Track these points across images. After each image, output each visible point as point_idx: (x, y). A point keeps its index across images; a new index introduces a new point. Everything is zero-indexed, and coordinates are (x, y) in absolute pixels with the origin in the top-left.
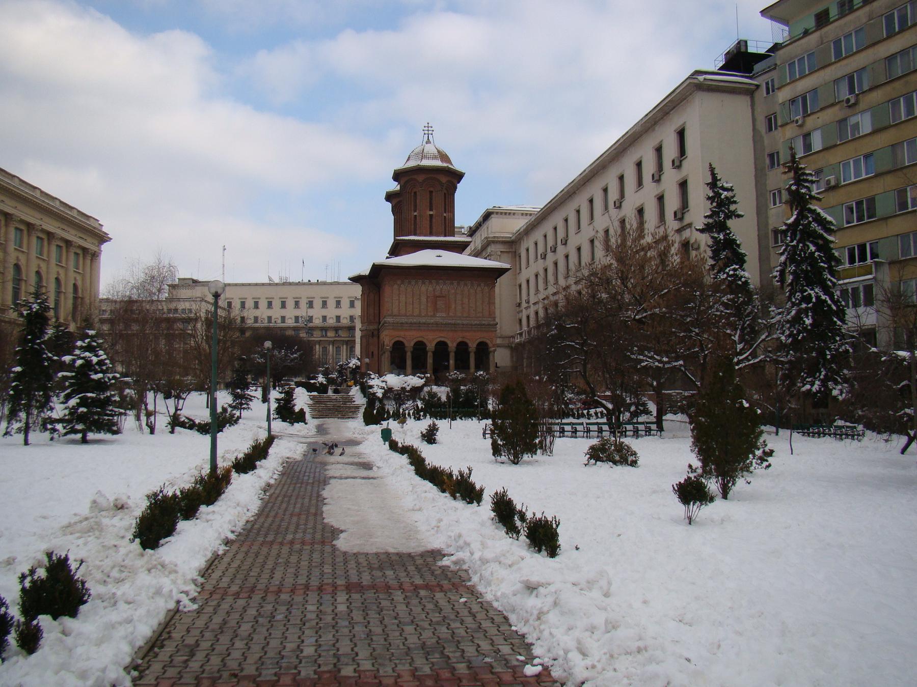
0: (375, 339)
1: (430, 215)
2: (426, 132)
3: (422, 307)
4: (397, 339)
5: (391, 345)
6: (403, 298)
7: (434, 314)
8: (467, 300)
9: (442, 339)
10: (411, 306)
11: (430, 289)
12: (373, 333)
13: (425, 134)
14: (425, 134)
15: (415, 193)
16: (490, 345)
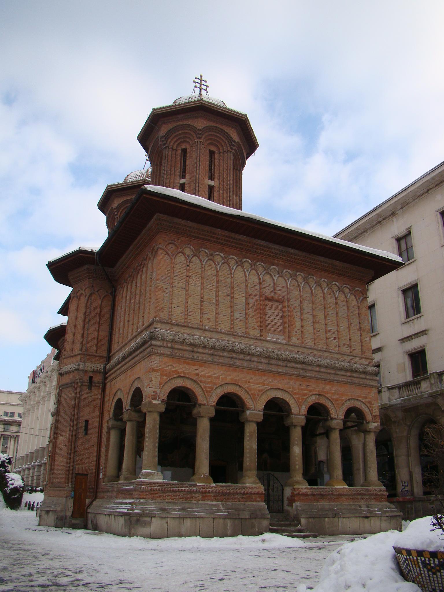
0: (96, 392)
1: (209, 186)
2: (198, 85)
3: (237, 315)
4: (178, 383)
5: (164, 394)
6: (195, 287)
7: (261, 335)
8: (323, 317)
9: (279, 395)
10: (213, 308)
11: (253, 279)
12: (91, 378)
13: (195, 87)
14: (195, 87)
15: (184, 151)
16: (369, 417)
